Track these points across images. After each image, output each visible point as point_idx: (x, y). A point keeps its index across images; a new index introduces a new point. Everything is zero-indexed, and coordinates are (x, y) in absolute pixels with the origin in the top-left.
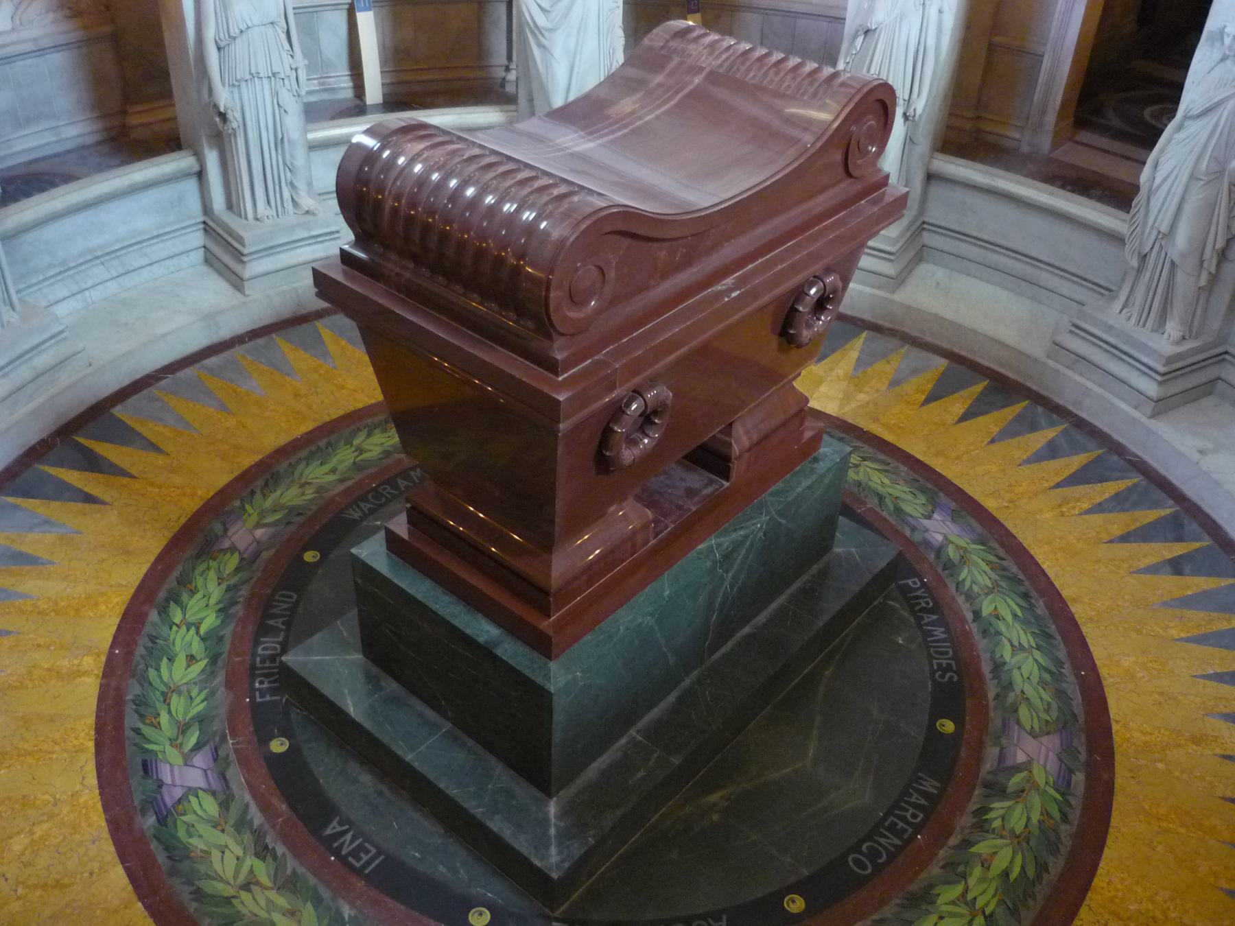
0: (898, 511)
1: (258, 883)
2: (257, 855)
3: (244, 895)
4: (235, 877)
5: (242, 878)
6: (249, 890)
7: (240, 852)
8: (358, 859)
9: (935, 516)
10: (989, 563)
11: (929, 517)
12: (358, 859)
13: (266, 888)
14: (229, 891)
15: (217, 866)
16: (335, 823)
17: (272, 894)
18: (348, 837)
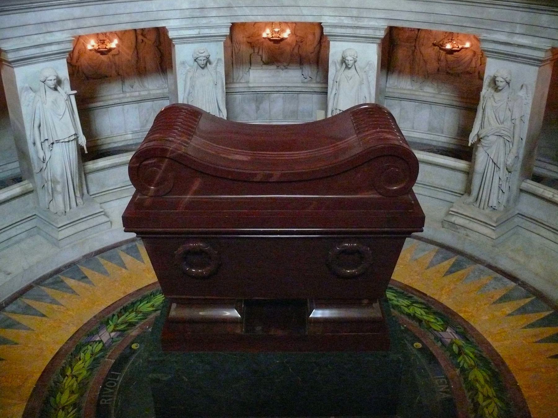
0: (101, 350)
1: (484, 396)
2: (479, 404)
3: (491, 395)
4: (489, 404)
5: (489, 401)
6: (488, 395)
7: (485, 409)
8: (444, 382)
9: (98, 339)
10: (119, 317)
11: (100, 341)
12: (444, 382)
13: (482, 393)
14: (496, 400)
15: (496, 409)
16: (444, 397)
17: (480, 389)
18: (442, 390)
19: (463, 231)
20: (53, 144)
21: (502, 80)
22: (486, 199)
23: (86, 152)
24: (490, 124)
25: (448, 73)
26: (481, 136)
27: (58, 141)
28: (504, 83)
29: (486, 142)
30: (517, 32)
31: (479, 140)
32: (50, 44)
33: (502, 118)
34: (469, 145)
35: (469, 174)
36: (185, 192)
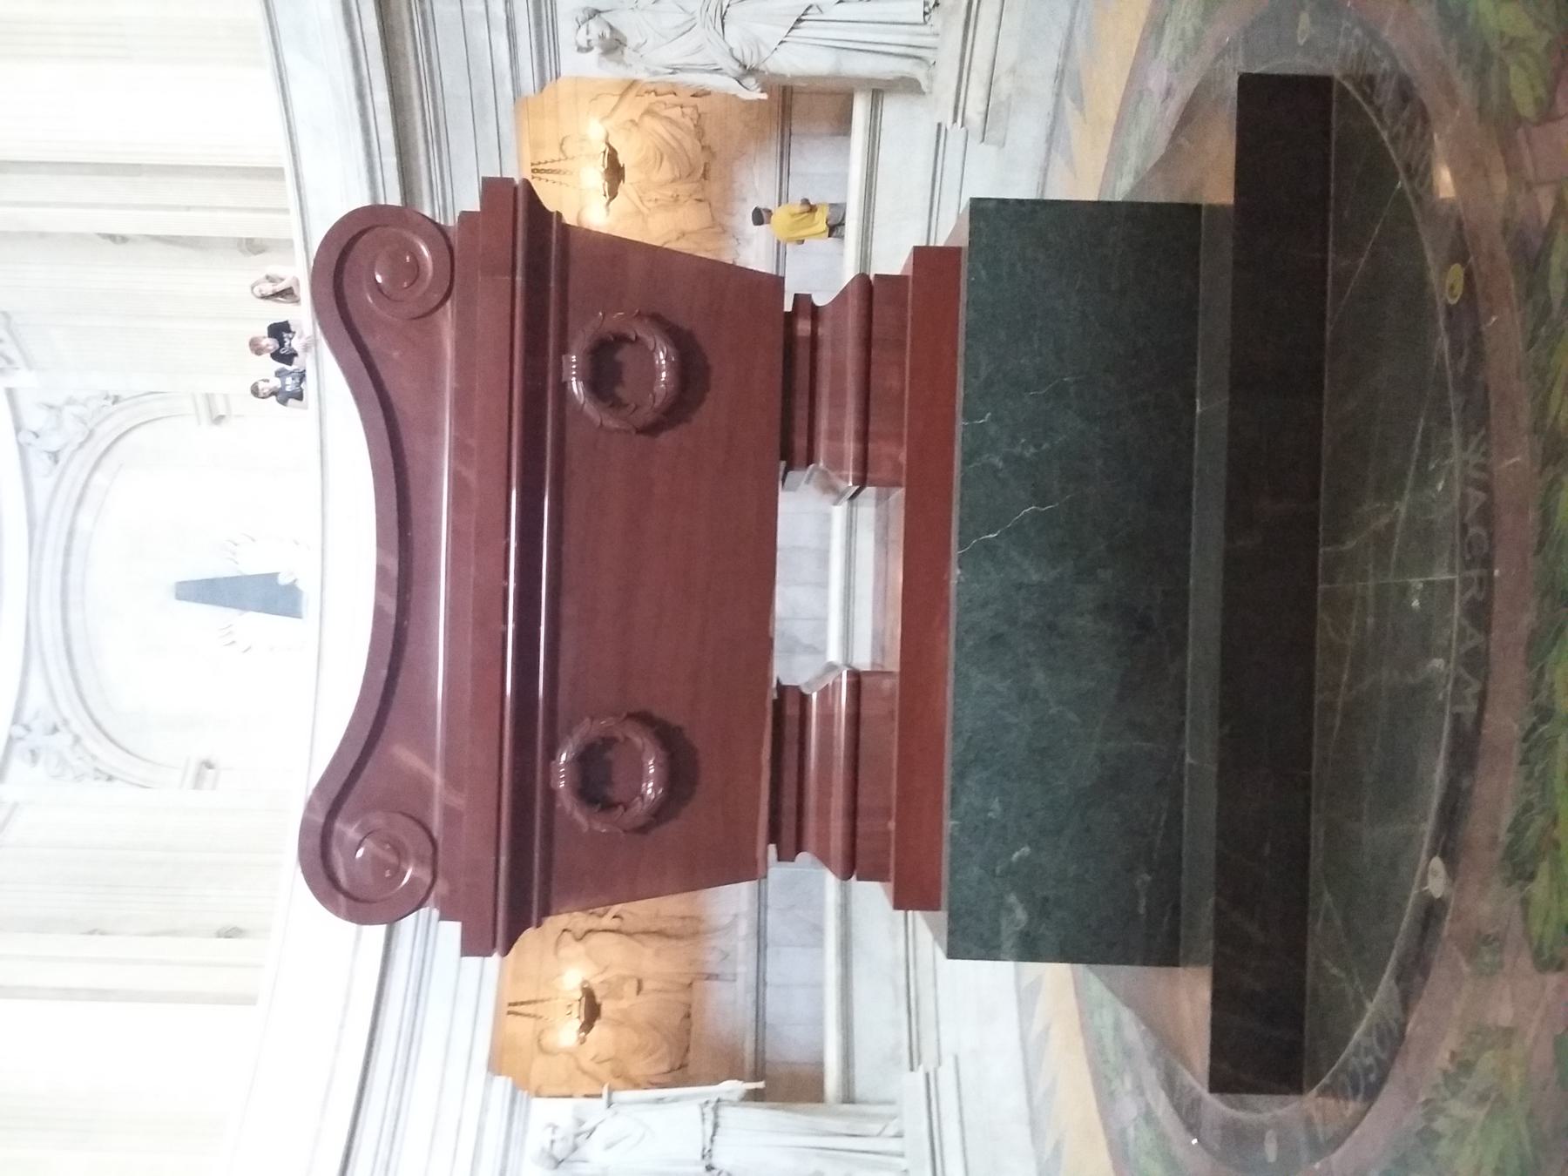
19: (1004, 85)
20: (709, 1168)
21: (584, 28)
22: (910, 34)
23: (761, 1085)
24: (700, 49)
25: (704, 176)
26: (740, 70)
27: (706, 1154)
28: (591, 23)
29: (747, 53)
30: (482, 8)
31: (748, 71)
32: (480, 1129)
33: (682, 18)
34: (764, 96)
35: (879, 91)
36: (422, 789)
